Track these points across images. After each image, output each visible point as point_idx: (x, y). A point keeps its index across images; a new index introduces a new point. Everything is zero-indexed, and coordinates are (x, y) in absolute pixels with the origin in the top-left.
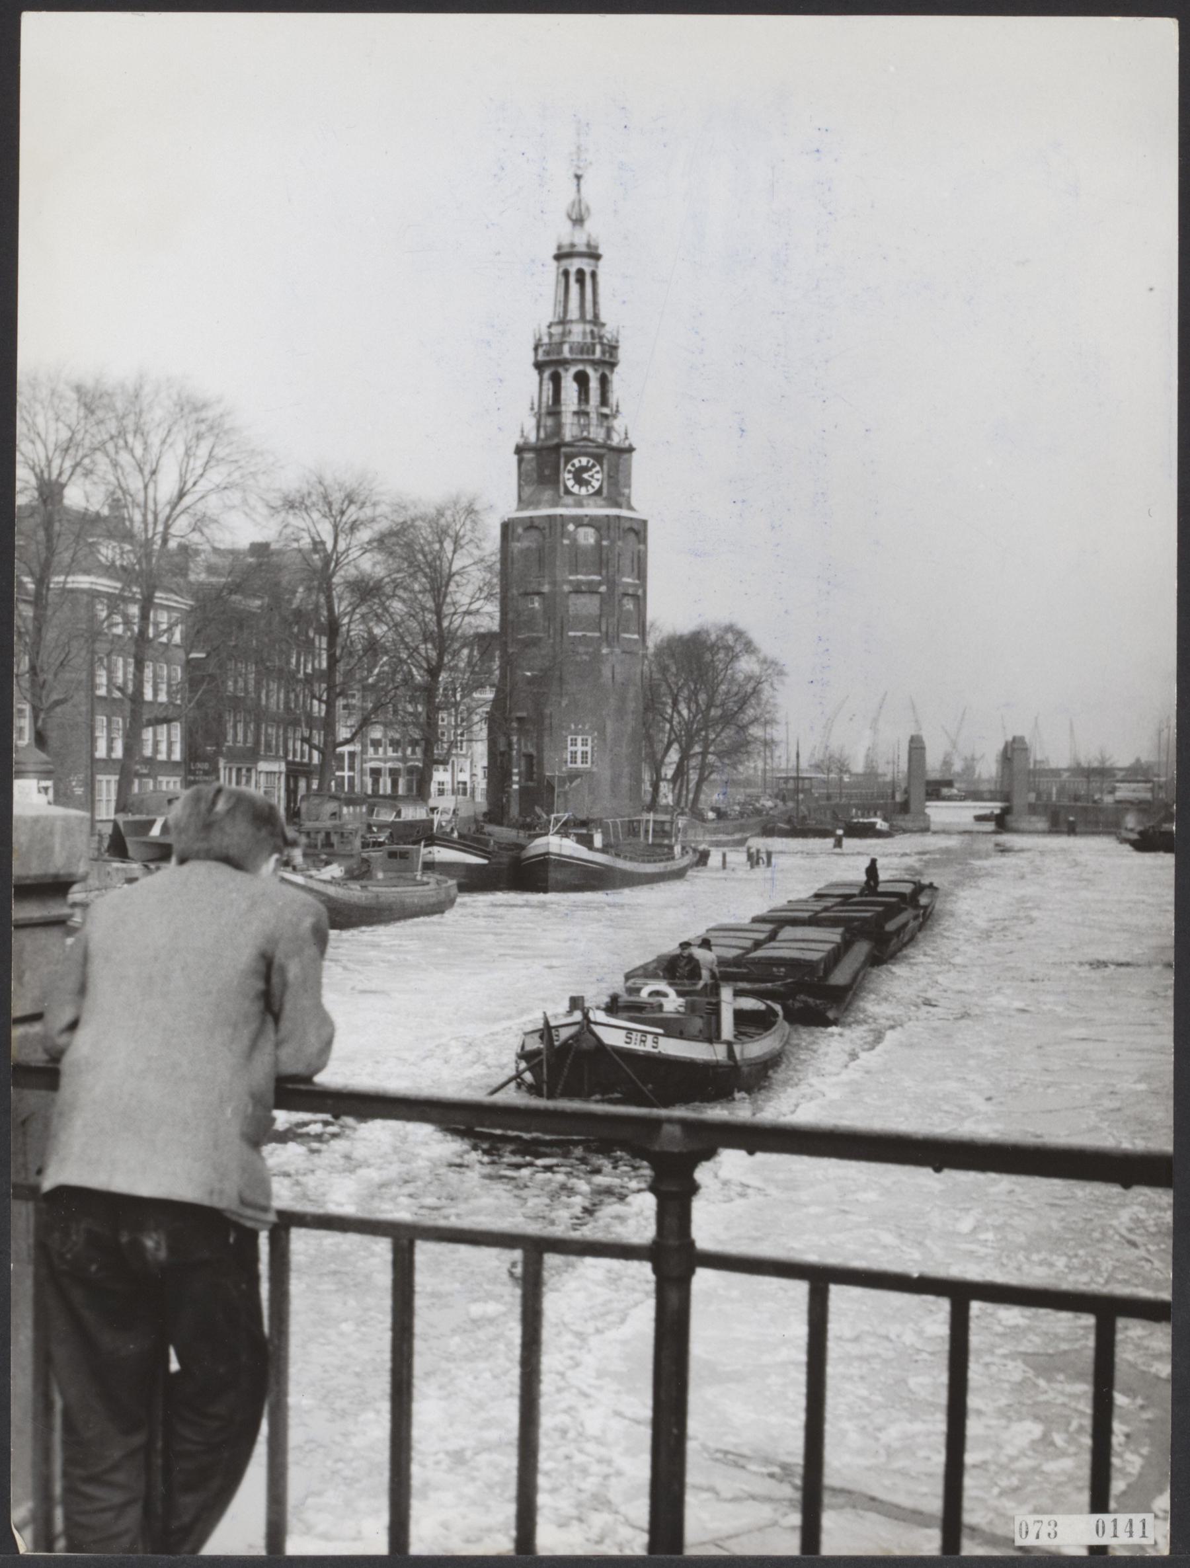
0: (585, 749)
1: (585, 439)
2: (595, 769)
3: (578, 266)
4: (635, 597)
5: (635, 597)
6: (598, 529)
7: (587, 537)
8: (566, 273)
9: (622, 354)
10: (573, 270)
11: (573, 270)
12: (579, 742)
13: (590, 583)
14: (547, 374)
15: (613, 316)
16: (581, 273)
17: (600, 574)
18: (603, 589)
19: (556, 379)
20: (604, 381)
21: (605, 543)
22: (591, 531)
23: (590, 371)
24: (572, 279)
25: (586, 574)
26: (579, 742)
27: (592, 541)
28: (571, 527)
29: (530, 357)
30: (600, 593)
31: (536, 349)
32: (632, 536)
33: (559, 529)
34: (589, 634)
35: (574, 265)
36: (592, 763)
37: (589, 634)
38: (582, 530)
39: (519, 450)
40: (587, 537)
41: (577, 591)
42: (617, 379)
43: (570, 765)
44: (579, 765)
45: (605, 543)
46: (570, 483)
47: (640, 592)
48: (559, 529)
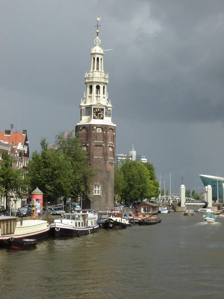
1: (99, 104)
6: (102, 129)
21: (104, 132)
22: (100, 129)
23: (100, 85)
27: (101, 131)
28: (95, 128)
32: (111, 130)
38: (98, 129)
40: (99, 131)
44: (97, 194)
45: (104, 132)
46: (95, 115)
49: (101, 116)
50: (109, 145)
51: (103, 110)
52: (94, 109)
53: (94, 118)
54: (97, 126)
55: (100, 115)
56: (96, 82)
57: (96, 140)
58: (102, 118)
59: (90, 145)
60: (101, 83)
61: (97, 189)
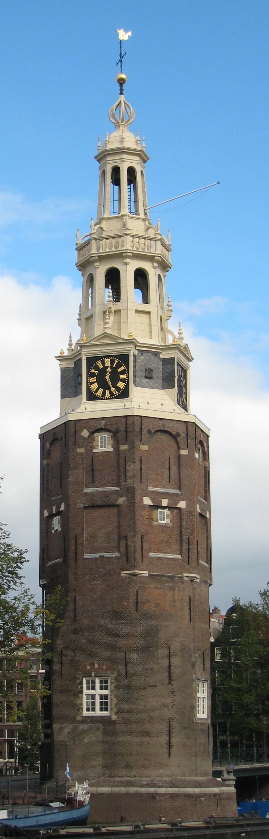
0: (105, 692)
1: (106, 336)
2: (114, 717)
6: (115, 435)
7: (104, 444)
12: (98, 685)
13: (105, 494)
17: (118, 485)
18: (121, 501)
22: (107, 436)
25: (103, 486)
26: (98, 685)
27: (109, 448)
30: (118, 506)
33: (72, 439)
34: (106, 555)
36: (111, 709)
37: (106, 555)
38: (99, 437)
40: (104, 444)
41: (93, 507)
43: (85, 713)
44: (98, 713)
46: (94, 387)
47: (182, 504)
48: (72, 439)
49: (121, 385)
50: (147, 501)
51: (124, 358)
52: (92, 361)
53: (92, 396)
54: (97, 426)
55: (115, 378)
56: (102, 258)
57: (93, 484)
58: (124, 394)
59: (67, 505)
60: (119, 256)
61: (98, 692)
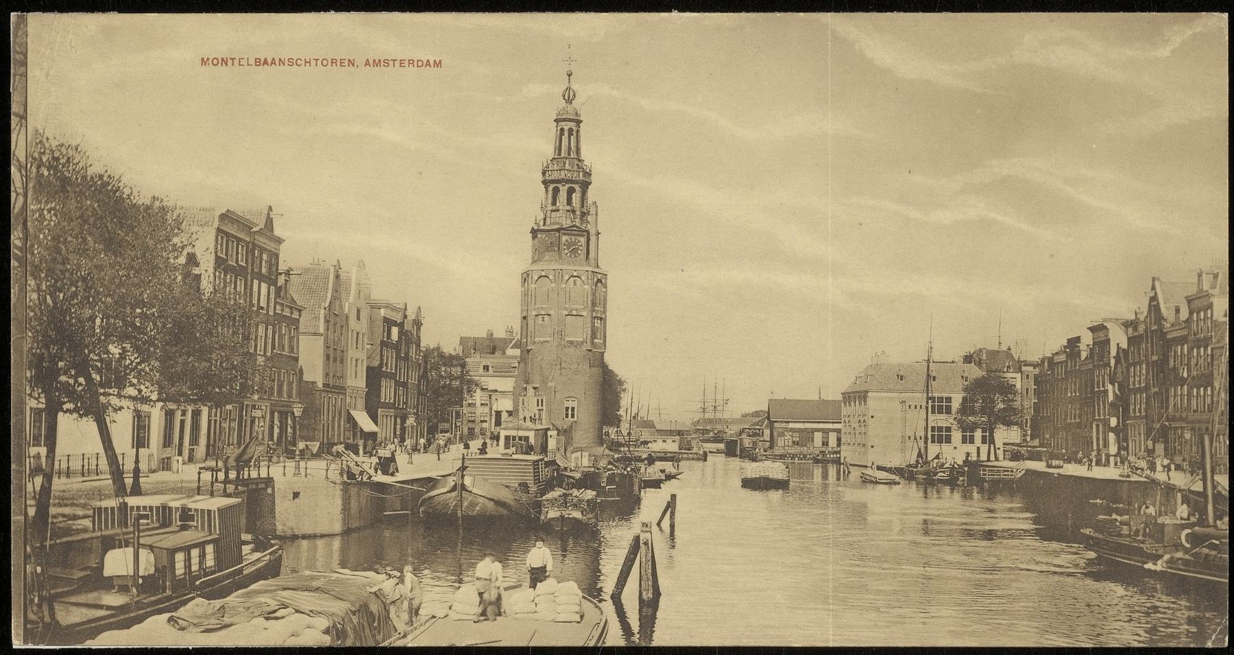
3: (569, 128)
4: (601, 319)
5: (601, 319)
8: (562, 130)
9: (593, 178)
10: (566, 128)
11: (566, 128)
14: (551, 187)
15: (590, 155)
16: (571, 130)
19: (556, 191)
20: (584, 193)
24: (566, 134)
29: (541, 178)
31: (544, 173)
35: (567, 126)
39: (534, 232)
42: (591, 190)
